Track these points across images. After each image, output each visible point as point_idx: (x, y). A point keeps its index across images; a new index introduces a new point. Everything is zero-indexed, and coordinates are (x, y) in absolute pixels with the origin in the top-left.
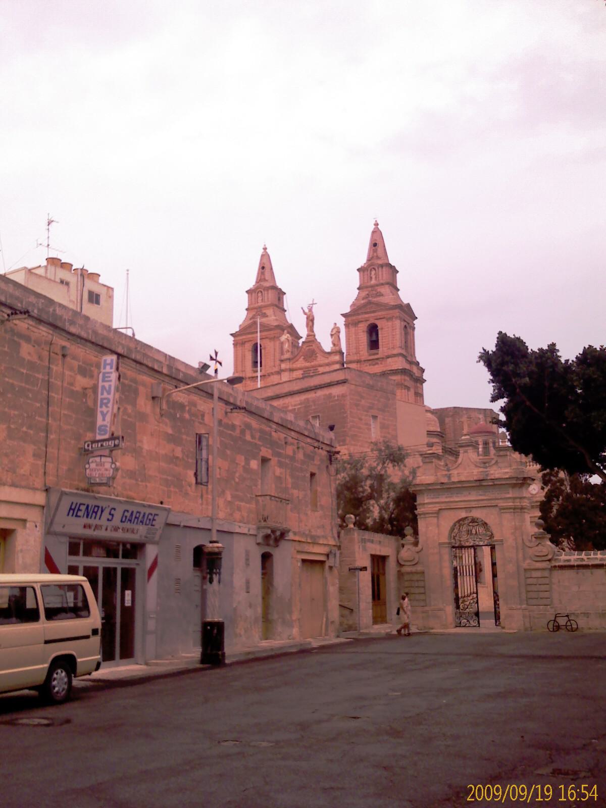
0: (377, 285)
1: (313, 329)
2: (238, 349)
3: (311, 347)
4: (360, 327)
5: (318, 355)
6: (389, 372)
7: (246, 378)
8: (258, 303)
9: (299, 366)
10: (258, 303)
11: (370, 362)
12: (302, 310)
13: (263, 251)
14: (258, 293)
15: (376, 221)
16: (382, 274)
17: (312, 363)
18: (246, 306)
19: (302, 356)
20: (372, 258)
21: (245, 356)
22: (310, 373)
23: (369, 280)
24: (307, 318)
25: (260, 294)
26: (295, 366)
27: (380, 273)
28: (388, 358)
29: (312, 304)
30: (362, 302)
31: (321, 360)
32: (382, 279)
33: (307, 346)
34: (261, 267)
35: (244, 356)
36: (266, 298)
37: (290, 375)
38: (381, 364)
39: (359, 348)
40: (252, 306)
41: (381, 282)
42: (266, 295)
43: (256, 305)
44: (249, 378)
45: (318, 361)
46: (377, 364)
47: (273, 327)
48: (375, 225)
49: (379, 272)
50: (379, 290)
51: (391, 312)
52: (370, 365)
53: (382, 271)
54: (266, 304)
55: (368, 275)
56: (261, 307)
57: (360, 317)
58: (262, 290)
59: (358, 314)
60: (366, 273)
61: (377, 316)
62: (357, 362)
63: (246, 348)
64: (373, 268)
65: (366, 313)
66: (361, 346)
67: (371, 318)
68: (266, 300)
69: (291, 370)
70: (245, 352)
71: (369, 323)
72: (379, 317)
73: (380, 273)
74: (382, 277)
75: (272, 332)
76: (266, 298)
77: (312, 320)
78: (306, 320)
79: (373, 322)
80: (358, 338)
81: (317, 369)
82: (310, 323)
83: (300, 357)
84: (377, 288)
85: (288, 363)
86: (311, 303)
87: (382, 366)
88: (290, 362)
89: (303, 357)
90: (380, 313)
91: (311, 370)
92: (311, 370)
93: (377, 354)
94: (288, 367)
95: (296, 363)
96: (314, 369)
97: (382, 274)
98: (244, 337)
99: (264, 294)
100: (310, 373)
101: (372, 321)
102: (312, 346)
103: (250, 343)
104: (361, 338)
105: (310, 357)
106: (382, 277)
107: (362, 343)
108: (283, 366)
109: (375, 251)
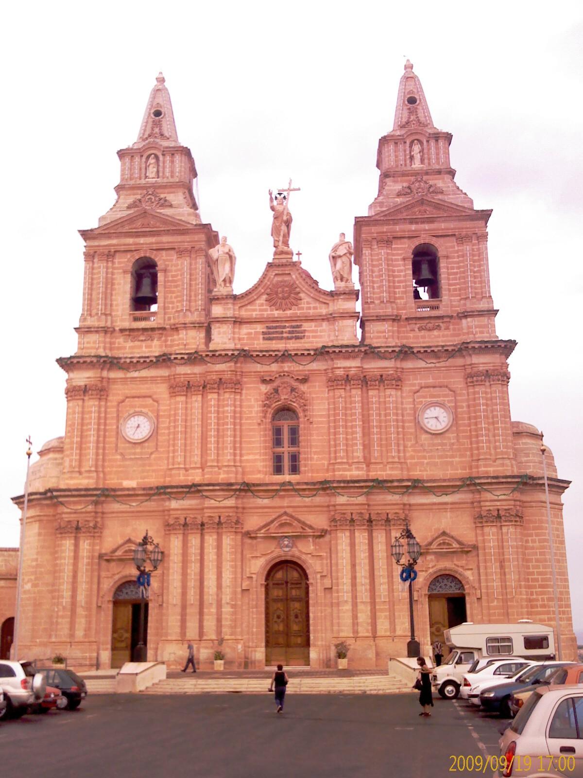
0: (427, 173)
1: (288, 241)
2: (96, 265)
3: (287, 278)
4: (396, 249)
5: (302, 295)
6: (477, 346)
7: (114, 330)
8: (146, 177)
9: (254, 314)
10: (146, 177)
11: (423, 323)
12: (269, 196)
13: (155, 83)
14: (148, 157)
15: (408, 61)
16: (438, 154)
17: (289, 312)
18: (117, 181)
19: (262, 294)
20: (407, 123)
21: (113, 284)
22: (282, 333)
23: (408, 162)
24: (276, 218)
25: (152, 161)
26: (244, 313)
27: (433, 151)
28: (466, 317)
29: (289, 190)
30: (399, 200)
31: (308, 305)
32: (438, 164)
33: (276, 275)
34: (153, 111)
35: (110, 283)
36: (167, 170)
37: (234, 333)
38: (447, 328)
39: (395, 293)
40: (132, 182)
42: (168, 164)
44: (122, 330)
45: (302, 308)
46: (438, 327)
47: (190, 227)
48: (406, 68)
49: (429, 149)
50: (431, 182)
51: (468, 224)
52: (420, 329)
53: (437, 148)
54: (165, 180)
55: (405, 151)
56: (155, 187)
57: (397, 228)
59: (395, 222)
60: (401, 147)
61: (438, 230)
62: (394, 320)
63: (117, 265)
64: (417, 140)
65: (412, 221)
66: (399, 287)
67: (424, 233)
68: (168, 174)
69: (238, 322)
70: (113, 274)
71: (417, 242)
72: (440, 233)
73: (433, 151)
74: (438, 159)
75: (187, 238)
76: (167, 170)
77: (288, 223)
78: (272, 219)
80: (393, 271)
81: (298, 327)
82: (284, 228)
84: (425, 178)
85: (230, 306)
86: (286, 187)
87: (446, 332)
88: (234, 304)
89: (265, 297)
90: (443, 225)
91: (285, 327)
92: (285, 327)
93: (437, 308)
94: (230, 313)
95: (249, 307)
96: (294, 324)
97: (438, 154)
98: (114, 241)
99: (164, 162)
100: (282, 333)
103: (129, 255)
104: (399, 271)
105: (284, 298)
106: (438, 159)
107: (399, 282)
109: (411, 112)
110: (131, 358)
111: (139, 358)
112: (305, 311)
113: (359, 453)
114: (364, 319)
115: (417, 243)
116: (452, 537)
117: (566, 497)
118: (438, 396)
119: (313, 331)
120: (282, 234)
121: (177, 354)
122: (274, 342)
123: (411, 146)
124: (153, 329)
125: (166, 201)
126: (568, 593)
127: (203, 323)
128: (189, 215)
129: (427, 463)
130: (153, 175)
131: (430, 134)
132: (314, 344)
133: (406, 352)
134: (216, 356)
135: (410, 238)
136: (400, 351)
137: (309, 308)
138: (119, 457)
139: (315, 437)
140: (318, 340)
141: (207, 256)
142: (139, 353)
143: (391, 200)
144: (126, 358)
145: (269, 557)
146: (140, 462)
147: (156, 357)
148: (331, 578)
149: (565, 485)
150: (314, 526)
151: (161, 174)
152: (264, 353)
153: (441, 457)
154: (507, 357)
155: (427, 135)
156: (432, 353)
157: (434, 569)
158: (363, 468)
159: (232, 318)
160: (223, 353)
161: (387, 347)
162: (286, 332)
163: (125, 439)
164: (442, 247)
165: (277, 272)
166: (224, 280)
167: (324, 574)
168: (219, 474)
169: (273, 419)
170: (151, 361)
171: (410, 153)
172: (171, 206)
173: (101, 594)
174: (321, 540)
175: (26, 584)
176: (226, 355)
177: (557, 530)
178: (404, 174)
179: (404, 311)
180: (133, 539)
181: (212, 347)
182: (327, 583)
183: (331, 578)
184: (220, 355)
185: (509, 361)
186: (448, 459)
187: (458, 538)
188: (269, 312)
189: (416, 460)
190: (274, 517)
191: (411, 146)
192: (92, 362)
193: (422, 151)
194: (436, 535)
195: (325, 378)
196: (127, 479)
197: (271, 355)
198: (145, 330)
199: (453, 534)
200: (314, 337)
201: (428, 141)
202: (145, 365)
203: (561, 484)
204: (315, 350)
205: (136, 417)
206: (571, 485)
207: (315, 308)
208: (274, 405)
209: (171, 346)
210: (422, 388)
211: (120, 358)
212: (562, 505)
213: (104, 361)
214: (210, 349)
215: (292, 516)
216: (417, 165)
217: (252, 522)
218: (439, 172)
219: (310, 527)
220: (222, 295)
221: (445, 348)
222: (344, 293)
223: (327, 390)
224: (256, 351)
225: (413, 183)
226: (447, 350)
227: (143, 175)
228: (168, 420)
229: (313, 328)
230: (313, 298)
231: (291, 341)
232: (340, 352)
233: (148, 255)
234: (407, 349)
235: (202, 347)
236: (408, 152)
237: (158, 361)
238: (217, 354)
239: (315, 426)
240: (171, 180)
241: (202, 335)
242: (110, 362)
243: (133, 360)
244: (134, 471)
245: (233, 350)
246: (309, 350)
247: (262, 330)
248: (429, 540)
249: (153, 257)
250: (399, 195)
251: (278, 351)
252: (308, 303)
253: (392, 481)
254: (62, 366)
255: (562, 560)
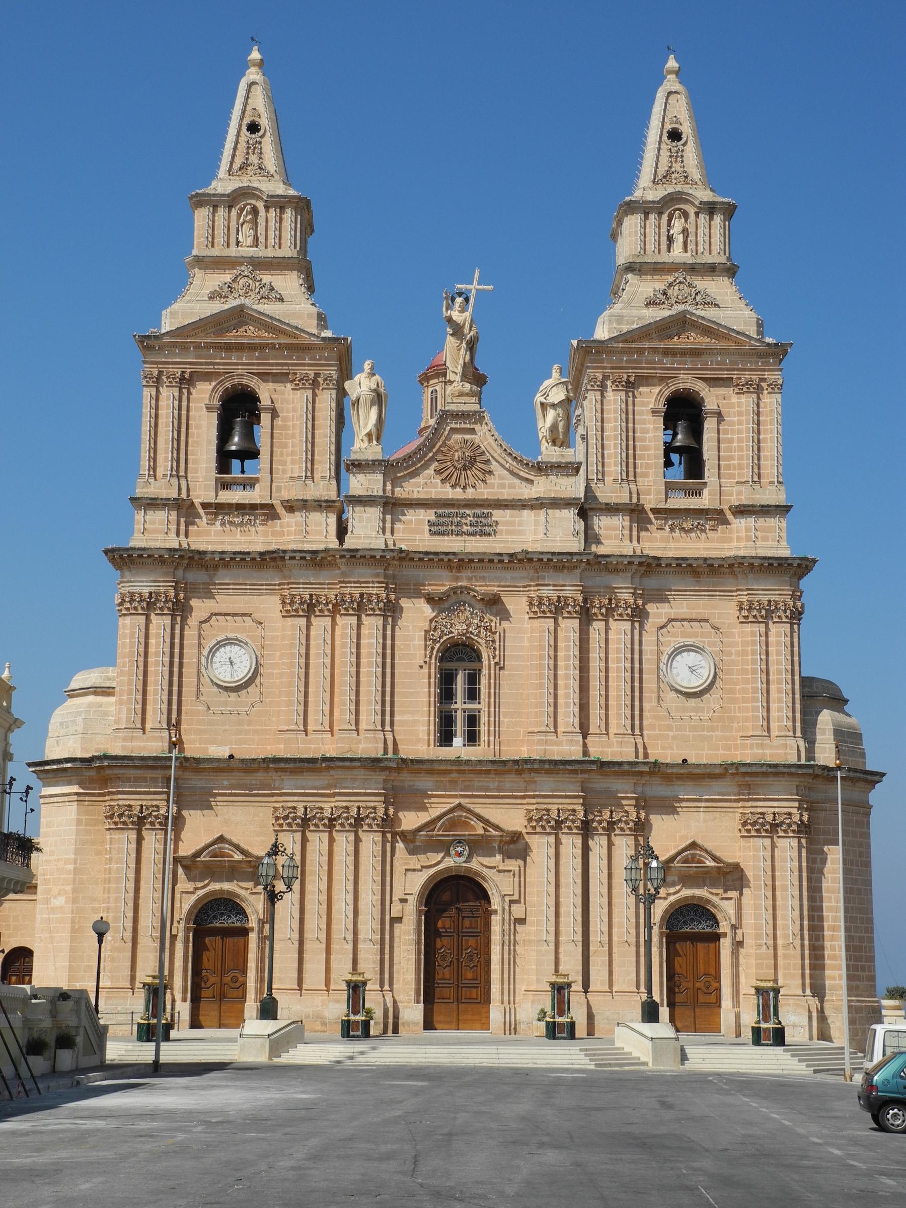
10: (238, 243)
23: (664, 247)
34: (246, 121)
40: (216, 252)
41: (708, 259)
43: (233, 251)
58: (260, 205)
64: (679, 209)
79: (688, 386)
83: (426, 466)
101: (686, 381)
102: (472, 431)
108: (358, 484)
110: (223, 553)
111: (235, 553)
112: (496, 490)
113: (569, 717)
114: (586, 506)
115: (673, 388)
116: (706, 851)
117: (876, 796)
118: (695, 635)
119: (508, 523)
120: (461, 362)
121: (294, 551)
122: (446, 538)
123: (670, 221)
124: (253, 507)
125: (272, 289)
126: (871, 940)
127: (334, 501)
128: (310, 316)
129: (674, 738)
130: (250, 241)
131: (701, 203)
132: (510, 545)
133: (649, 565)
134: (354, 556)
135: (662, 379)
136: (640, 564)
137: (502, 486)
138: (202, 708)
139: (506, 690)
140: (516, 538)
141: (342, 393)
142: (230, 543)
143: (634, 312)
144: (213, 552)
145: (432, 871)
146: (235, 717)
147: (262, 554)
148: (525, 904)
149: (876, 778)
150: (502, 826)
151: (262, 239)
152: (431, 557)
153: (694, 728)
154: (800, 578)
155: (697, 203)
156: (688, 568)
157: (677, 896)
158: (578, 741)
159: (381, 497)
160: (368, 554)
161: (621, 556)
162: (466, 524)
163: (212, 681)
164: (711, 398)
165: (453, 426)
166: (369, 435)
167: (516, 897)
168: (359, 742)
169: (441, 660)
170: (254, 559)
171: (668, 231)
172: (281, 300)
173: (177, 917)
174: (512, 846)
175: (55, 898)
176: (373, 557)
177: (860, 845)
178: (658, 269)
179: (648, 497)
180: (227, 836)
181: (350, 542)
182: (518, 911)
183: (525, 904)
184: (363, 557)
185: (804, 583)
186: (705, 733)
187: (714, 852)
188: (439, 489)
189: (657, 732)
190: (443, 810)
191: (670, 221)
192: (160, 556)
193: (685, 232)
194: (683, 845)
195: (525, 599)
196: (214, 742)
197: (442, 560)
198: (241, 508)
199: (708, 845)
200: (509, 532)
201: (697, 214)
202: (242, 563)
203: (869, 777)
204: (511, 555)
205: (228, 648)
206: (884, 779)
207: (512, 486)
208: (445, 638)
209: (282, 534)
210: (671, 620)
211: (205, 552)
212: (871, 807)
213: (181, 557)
214: (344, 547)
215: (469, 811)
216: (677, 254)
217: (410, 820)
218: (711, 270)
219: (497, 828)
220: (367, 460)
221: (708, 562)
222: (559, 466)
223: (527, 616)
224: (420, 552)
225: (670, 285)
226: (712, 565)
227: (233, 241)
228: (278, 654)
229: (508, 518)
230: (508, 470)
231: (472, 538)
232: (549, 560)
233: (244, 381)
234: (651, 561)
235: (334, 543)
236: (664, 229)
237: (262, 560)
238: (359, 554)
239: (507, 673)
240: (280, 253)
241: (332, 519)
242: (190, 558)
243: (224, 556)
244: (225, 730)
245: (383, 550)
246: (500, 554)
247: (427, 518)
248: (673, 852)
249: (252, 384)
250: (650, 303)
251: (454, 554)
252: (501, 477)
253: (620, 764)
254: (113, 560)
255: (866, 890)
